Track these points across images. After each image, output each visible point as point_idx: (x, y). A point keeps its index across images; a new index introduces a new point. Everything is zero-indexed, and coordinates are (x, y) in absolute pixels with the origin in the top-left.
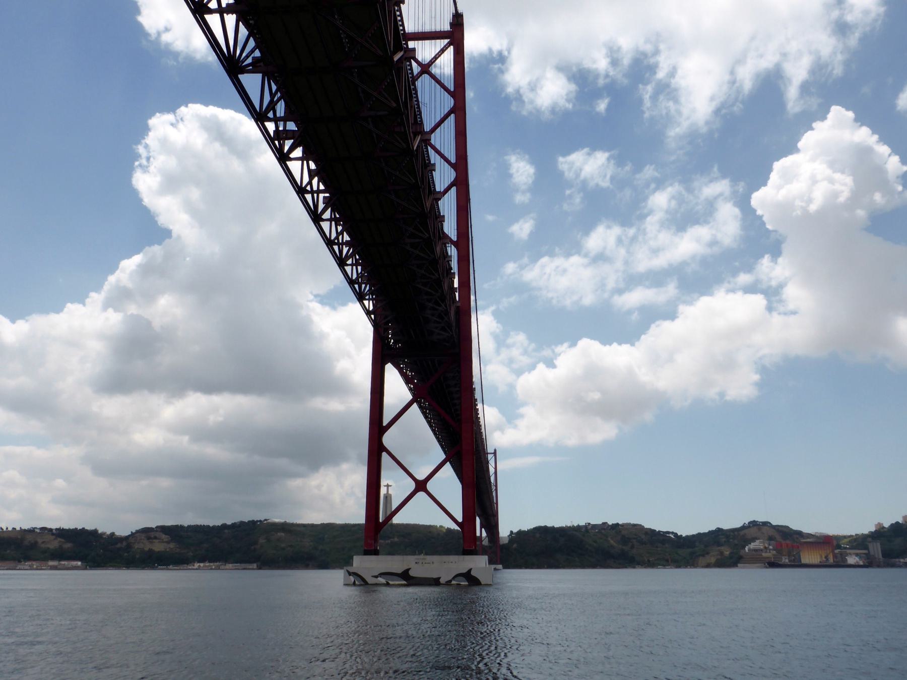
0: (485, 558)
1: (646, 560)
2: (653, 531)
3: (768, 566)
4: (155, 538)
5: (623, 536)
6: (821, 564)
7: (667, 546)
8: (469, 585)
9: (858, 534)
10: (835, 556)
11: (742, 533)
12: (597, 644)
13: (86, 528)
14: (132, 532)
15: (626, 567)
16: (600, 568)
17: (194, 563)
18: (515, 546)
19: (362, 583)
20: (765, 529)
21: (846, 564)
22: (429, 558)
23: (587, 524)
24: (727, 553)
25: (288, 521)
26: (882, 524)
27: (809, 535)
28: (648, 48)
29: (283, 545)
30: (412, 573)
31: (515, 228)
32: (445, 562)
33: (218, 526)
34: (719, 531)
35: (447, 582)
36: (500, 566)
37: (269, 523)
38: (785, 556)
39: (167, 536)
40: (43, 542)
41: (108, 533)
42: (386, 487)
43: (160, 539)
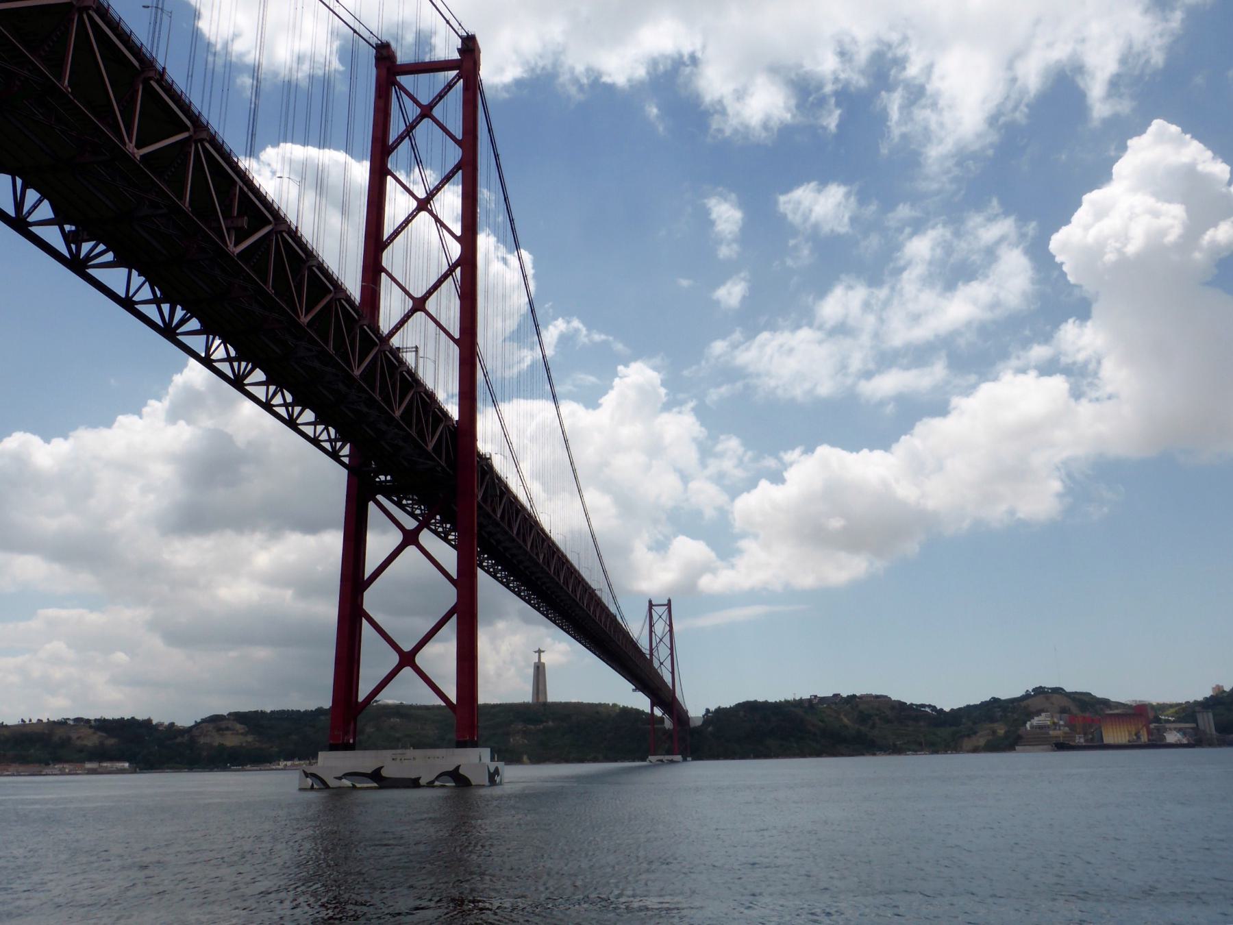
0: (486, 753)
1: (891, 744)
3: (1056, 748)
4: (227, 729)
6: (1130, 744)
7: (922, 724)
10: (1150, 733)
11: (1023, 704)
13: (136, 718)
14: (196, 722)
15: (862, 754)
16: (825, 757)
17: (280, 761)
18: (710, 729)
19: (322, 787)
21: (1163, 743)
22: (411, 752)
23: (813, 697)
24: (1001, 732)
25: (404, 702)
26: (1222, 686)
27: (1119, 705)
28: (894, 37)
29: (397, 735)
30: (384, 773)
32: (429, 758)
33: (312, 711)
34: (995, 701)
35: (428, 783)
36: (679, 758)
37: (380, 705)
38: (1079, 734)
39: (243, 726)
40: (78, 738)
41: (166, 723)
42: (537, 654)
43: (233, 730)
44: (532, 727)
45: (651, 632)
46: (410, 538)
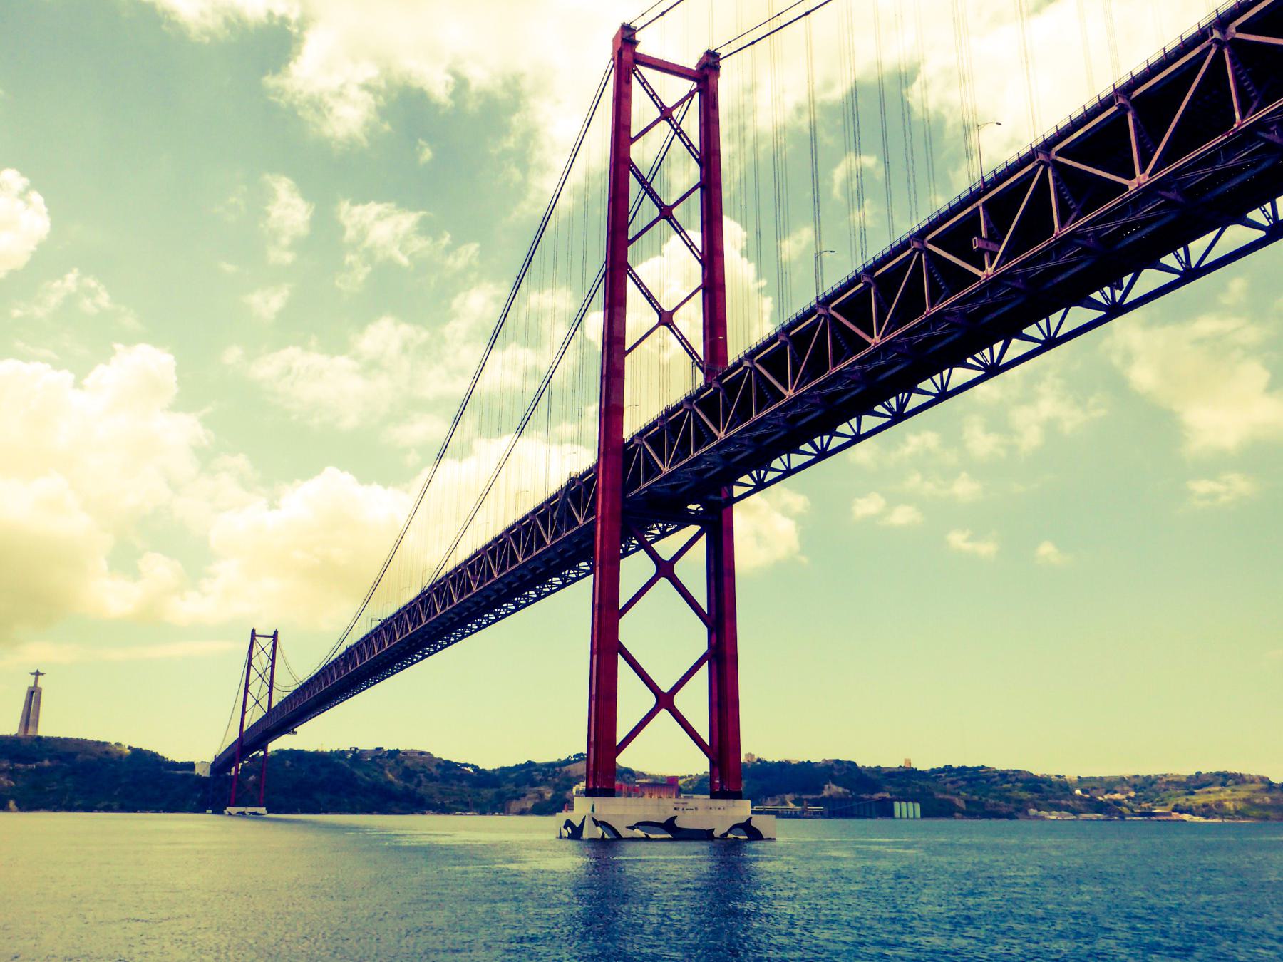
2: (448, 762)
5: (407, 768)
7: (464, 783)
9: (691, 775)
16: (376, 814)
19: (615, 837)
23: (353, 749)
24: (548, 796)
28: (501, 95)
30: (679, 823)
31: (256, 299)
34: (530, 764)
35: (721, 836)
36: (262, 810)
42: (34, 676)
44: (21, 766)
45: (250, 665)
46: (665, 569)
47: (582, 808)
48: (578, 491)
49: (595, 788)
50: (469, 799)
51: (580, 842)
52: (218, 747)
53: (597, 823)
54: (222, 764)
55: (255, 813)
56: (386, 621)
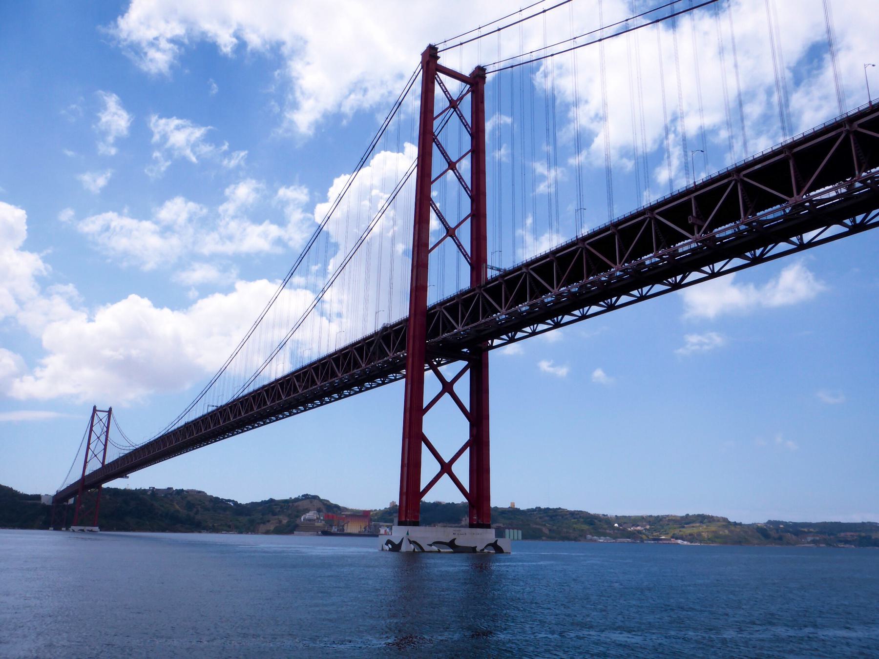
1: (211, 525)
2: (217, 498)
5: (189, 502)
7: (228, 513)
8: (496, 553)
12: (370, 601)
19: (420, 550)
20: (315, 502)
23: (152, 489)
24: (285, 522)
26: (395, 502)
27: (345, 509)
30: (457, 543)
32: (474, 534)
34: (272, 500)
35: (481, 550)
38: (335, 526)
46: (448, 387)
47: (398, 533)
48: (389, 335)
49: (406, 521)
50: (231, 523)
51: (399, 553)
52: (61, 483)
53: (411, 542)
54: (61, 497)
55: (91, 531)
56: (221, 407)
